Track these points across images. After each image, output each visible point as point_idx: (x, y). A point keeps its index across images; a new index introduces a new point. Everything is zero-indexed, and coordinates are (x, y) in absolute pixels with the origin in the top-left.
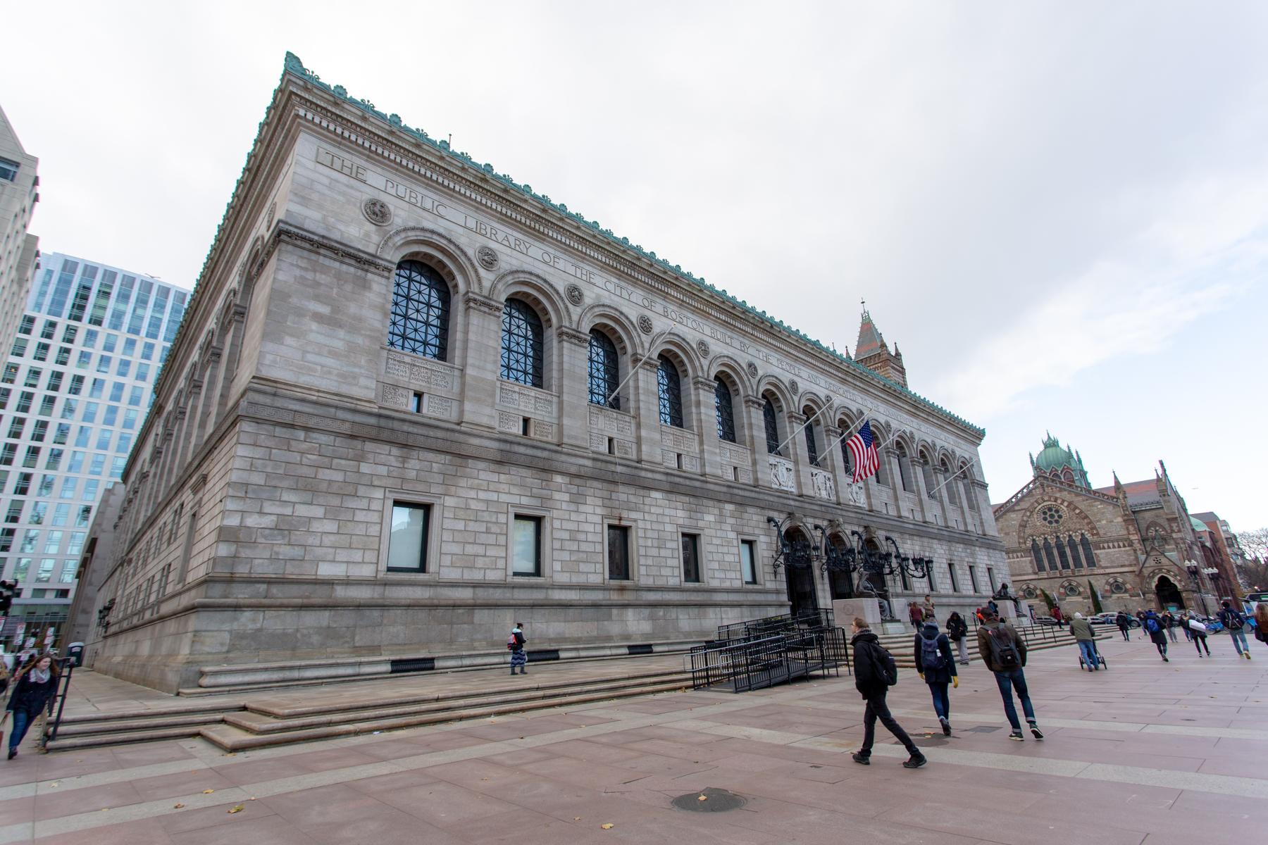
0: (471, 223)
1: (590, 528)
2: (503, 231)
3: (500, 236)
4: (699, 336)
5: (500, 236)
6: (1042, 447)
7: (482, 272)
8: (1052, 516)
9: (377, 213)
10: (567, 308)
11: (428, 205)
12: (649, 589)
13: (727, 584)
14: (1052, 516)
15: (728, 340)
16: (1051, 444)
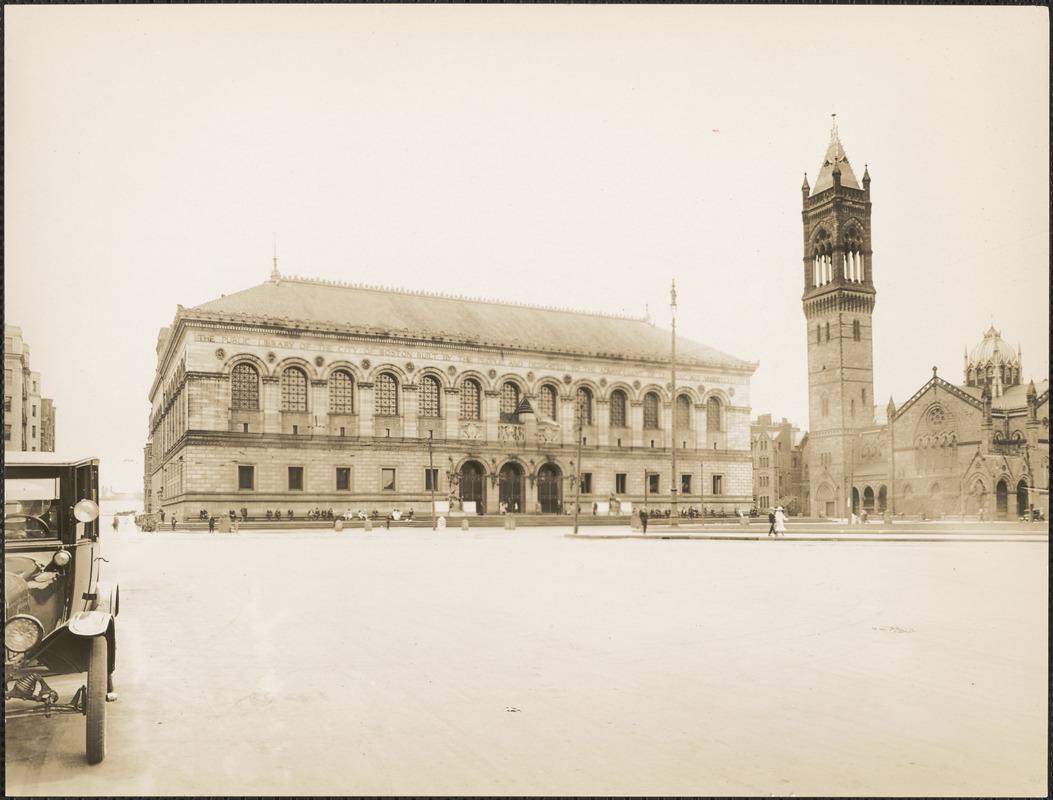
0: (262, 342)
1: (326, 470)
2: (279, 340)
3: (277, 344)
4: (407, 360)
5: (277, 344)
6: (983, 338)
7: (269, 365)
8: (937, 417)
9: (221, 353)
10: (315, 370)
11: (241, 341)
12: (359, 494)
13: (412, 492)
14: (937, 417)
15: (432, 356)
16: (993, 335)
